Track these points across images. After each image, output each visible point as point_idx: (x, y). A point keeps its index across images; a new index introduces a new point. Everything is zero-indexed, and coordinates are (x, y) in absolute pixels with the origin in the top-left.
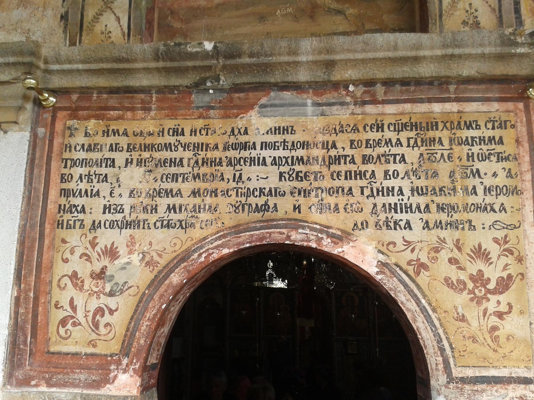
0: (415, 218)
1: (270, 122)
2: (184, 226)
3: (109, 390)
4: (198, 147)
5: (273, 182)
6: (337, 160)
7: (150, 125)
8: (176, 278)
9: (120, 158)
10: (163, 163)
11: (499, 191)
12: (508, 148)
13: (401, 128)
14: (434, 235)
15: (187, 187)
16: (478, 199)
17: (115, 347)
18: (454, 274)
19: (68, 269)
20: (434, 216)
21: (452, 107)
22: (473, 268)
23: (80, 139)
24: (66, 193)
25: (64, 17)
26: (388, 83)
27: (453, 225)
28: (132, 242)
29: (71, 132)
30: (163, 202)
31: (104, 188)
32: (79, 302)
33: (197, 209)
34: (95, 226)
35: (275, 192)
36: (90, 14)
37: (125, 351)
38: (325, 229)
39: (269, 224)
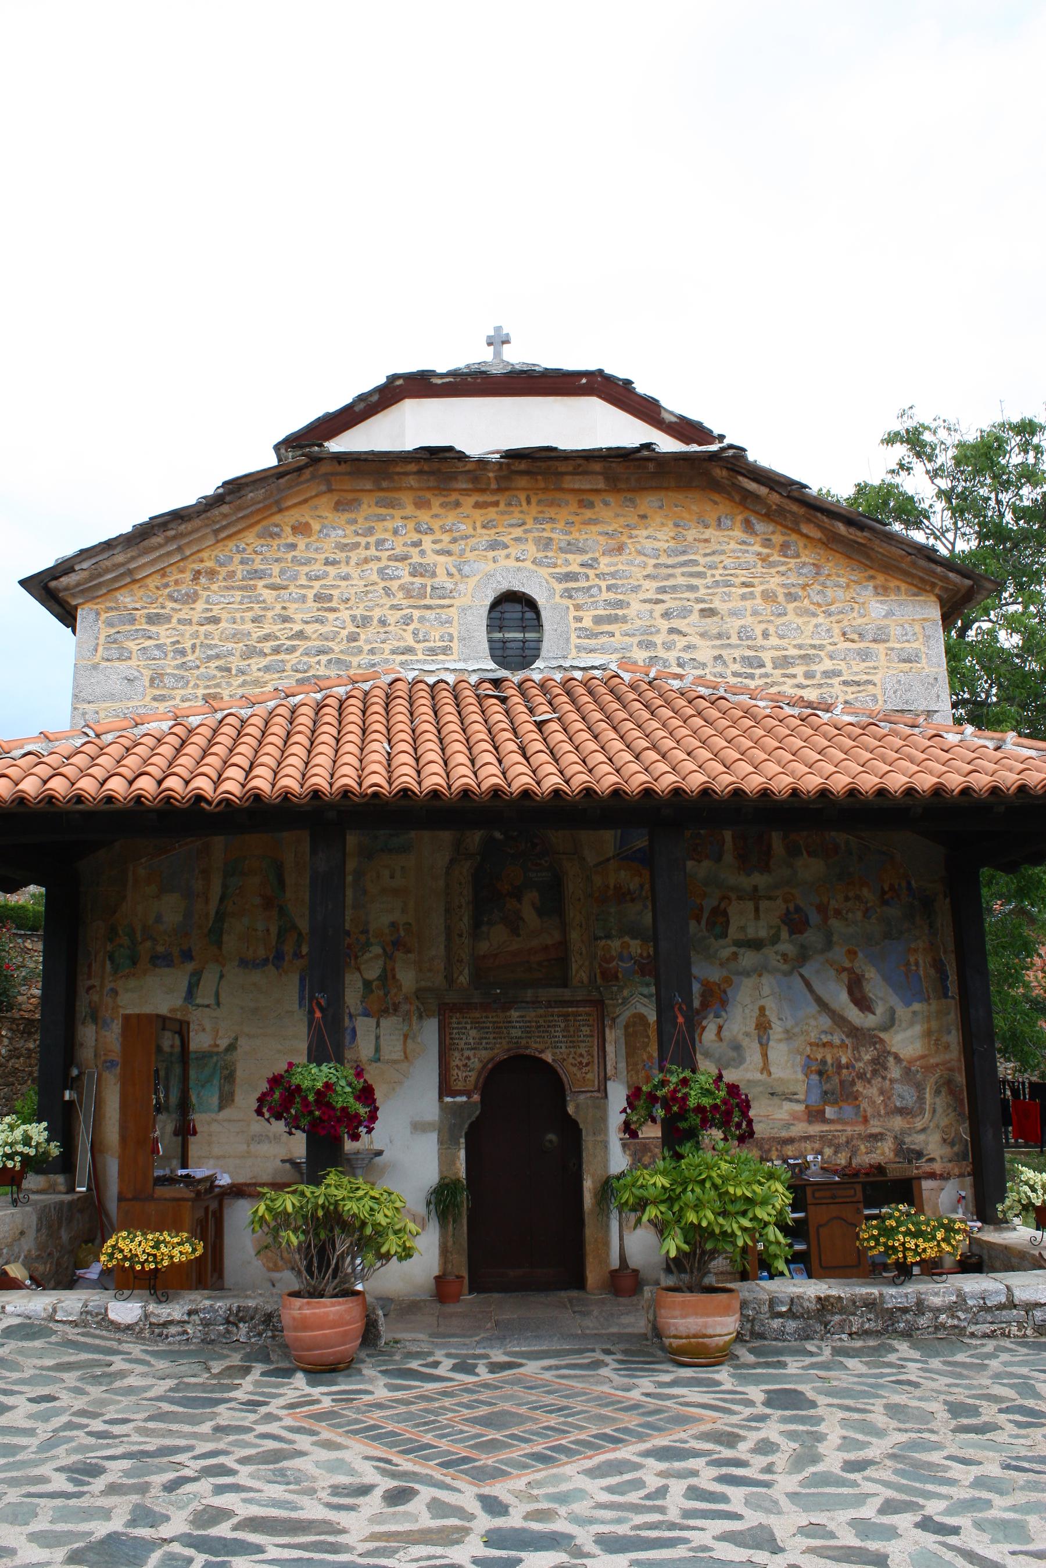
0: (563, 1045)
1: (517, 1014)
2: (492, 1049)
3: (472, 1100)
4: (494, 1022)
5: (520, 1034)
6: (539, 1027)
7: (477, 1015)
8: (490, 1066)
9: (468, 1026)
10: (483, 1028)
11: (587, 1036)
12: (591, 1022)
13: (559, 1016)
14: (567, 1051)
15: (492, 1036)
16: (582, 1038)
17: (472, 1087)
18: (574, 1062)
19: (454, 1064)
20: (569, 1044)
21: (574, 1009)
22: (579, 1060)
23: (454, 1020)
24: (452, 1039)
25: (446, 977)
26: (555, 1002)
27: (574, 1047)
28: (475, 1055)
29: (451, 1017)
30: (484, 1041)
31: (464, 1037)
32: (460, 1074)
33: (495, 1044)
34: (462, 1050)
35: (521, 1038)
36: (455, 976)
37: (475, 1088)
38: (536, 1049)
39: (518, 1048)
